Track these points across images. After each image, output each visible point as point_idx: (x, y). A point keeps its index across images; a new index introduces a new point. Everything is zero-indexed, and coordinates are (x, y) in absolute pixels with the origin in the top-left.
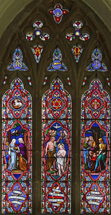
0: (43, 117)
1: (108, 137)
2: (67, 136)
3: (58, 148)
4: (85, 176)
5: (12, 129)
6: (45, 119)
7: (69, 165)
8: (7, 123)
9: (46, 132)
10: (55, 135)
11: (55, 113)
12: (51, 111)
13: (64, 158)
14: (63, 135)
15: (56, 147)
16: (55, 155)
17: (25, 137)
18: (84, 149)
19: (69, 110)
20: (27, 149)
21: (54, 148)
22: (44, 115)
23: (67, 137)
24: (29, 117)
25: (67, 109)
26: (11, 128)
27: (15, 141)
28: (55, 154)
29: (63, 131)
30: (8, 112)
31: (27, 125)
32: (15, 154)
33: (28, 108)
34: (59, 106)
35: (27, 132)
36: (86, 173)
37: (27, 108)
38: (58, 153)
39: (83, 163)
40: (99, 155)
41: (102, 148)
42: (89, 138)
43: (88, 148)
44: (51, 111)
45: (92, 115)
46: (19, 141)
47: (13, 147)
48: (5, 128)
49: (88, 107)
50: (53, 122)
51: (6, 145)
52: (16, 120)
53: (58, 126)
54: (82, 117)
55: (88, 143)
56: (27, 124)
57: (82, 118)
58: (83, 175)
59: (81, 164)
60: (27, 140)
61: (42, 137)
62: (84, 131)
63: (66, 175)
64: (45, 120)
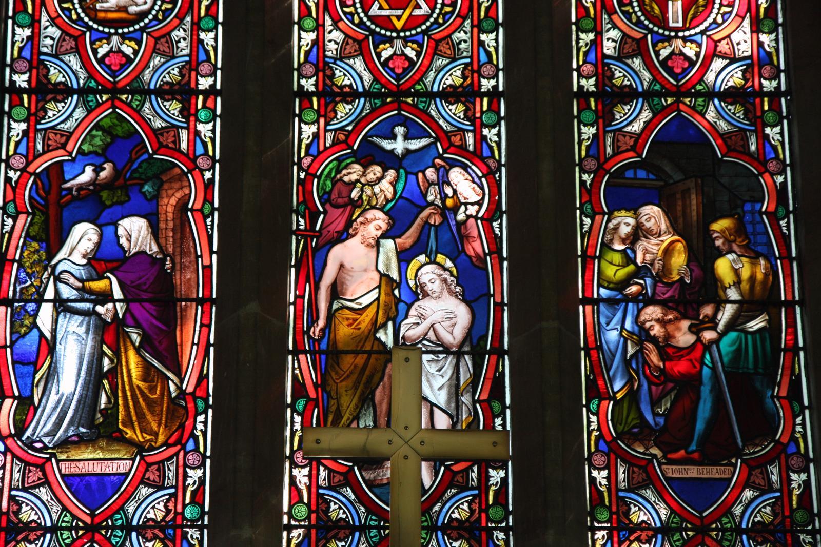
0: (303, 82)
1: (781, 211)
2: (472, 204)
3: (412, 283)
4: (623, 485)
5: (73, 160)
6: (313, 94)
7: (496, 406)
8: (41, 114)
9: (319, 178)
10: (388, 201)
11: (385, 55)
12: (359, 42)
13: (459, 355)
14: (444, 197)
15: (395, 275)
16: (386, 337)
17: (170, 209)
18: (604, 292)
19: (483, 37)
20: (181, 290)
21: (379, 287)
22: (309, 69)
23: (478, 212)
24: (201, 80)
25: (472, 26)
26: (69, 147)
27: (95, 238)
28: (390, 324)
29: (447, 172)
30: (46, 44)
31: (187, 128)
32: (87, 332)
33: (193, 23)
34: (417, 12)
35: (180, 180)
36: (629, 460)
37: (189, 19)
38: (410, 320)
39: (602, 390)
40: (722, 335)
41: (738, 283)
42: (637, 216)
43: (634, 289)
44: (359, 42)
45: (649, 65)
46: (123, 241)
47: (72, 280)
48: (22, 149)
49: (623, 12)
50: (375, 112)
51: (21, 266)
52: (105, 97)
53: (407, 137)
54: (583, 82)
55: (635, 252)
56: (188, 122)
57: (580, 87)
58: (604, 482)
59: (588, 402)
60: (183, 237)
61: (292, 211)
62: (598, 173)
63: (474, 475)
64: (315, 100)
